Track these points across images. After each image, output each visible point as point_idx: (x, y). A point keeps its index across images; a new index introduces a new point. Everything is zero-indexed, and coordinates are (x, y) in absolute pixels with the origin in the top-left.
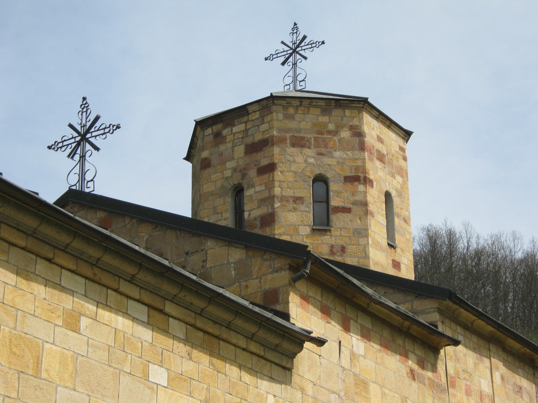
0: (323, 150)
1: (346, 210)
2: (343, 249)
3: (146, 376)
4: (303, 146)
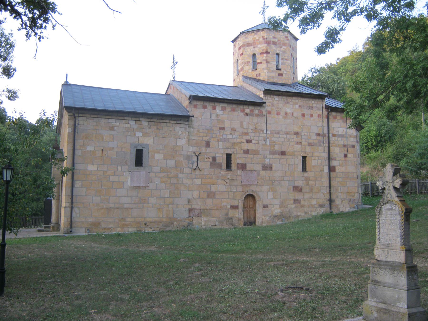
0: (255, 46)
1: (261, 63)
2: (260, 74)
3: (135, 135)
4: (250, 46)
